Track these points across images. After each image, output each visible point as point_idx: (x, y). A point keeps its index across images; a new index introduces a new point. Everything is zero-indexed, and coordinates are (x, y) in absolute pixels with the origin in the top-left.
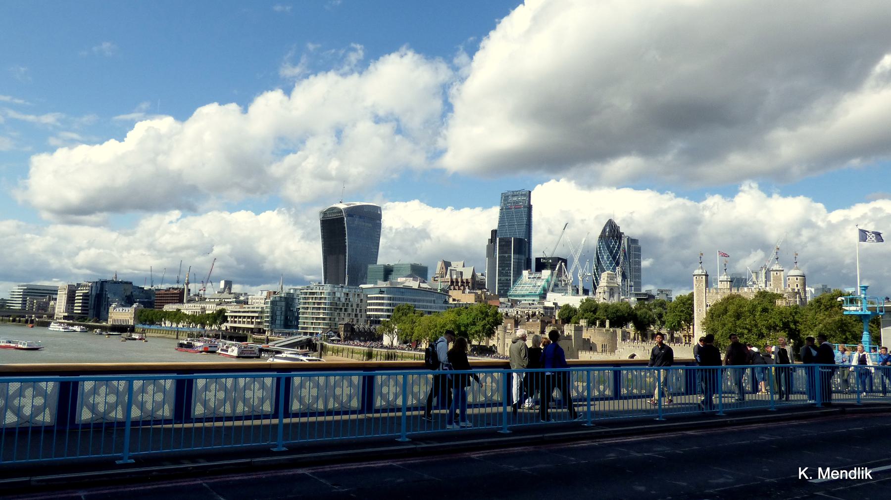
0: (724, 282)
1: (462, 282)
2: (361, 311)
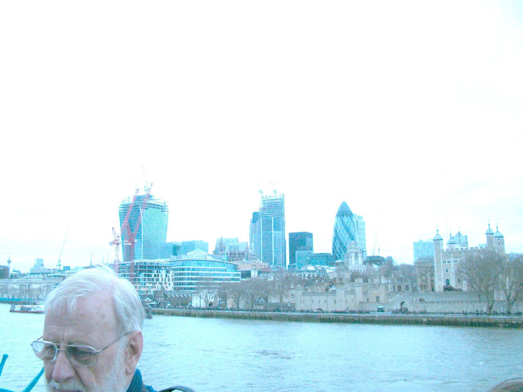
1: (239, 254)
2: (169, 280)
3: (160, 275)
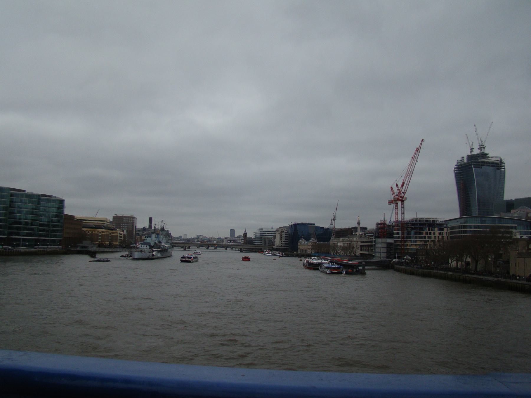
3: (432, 232)
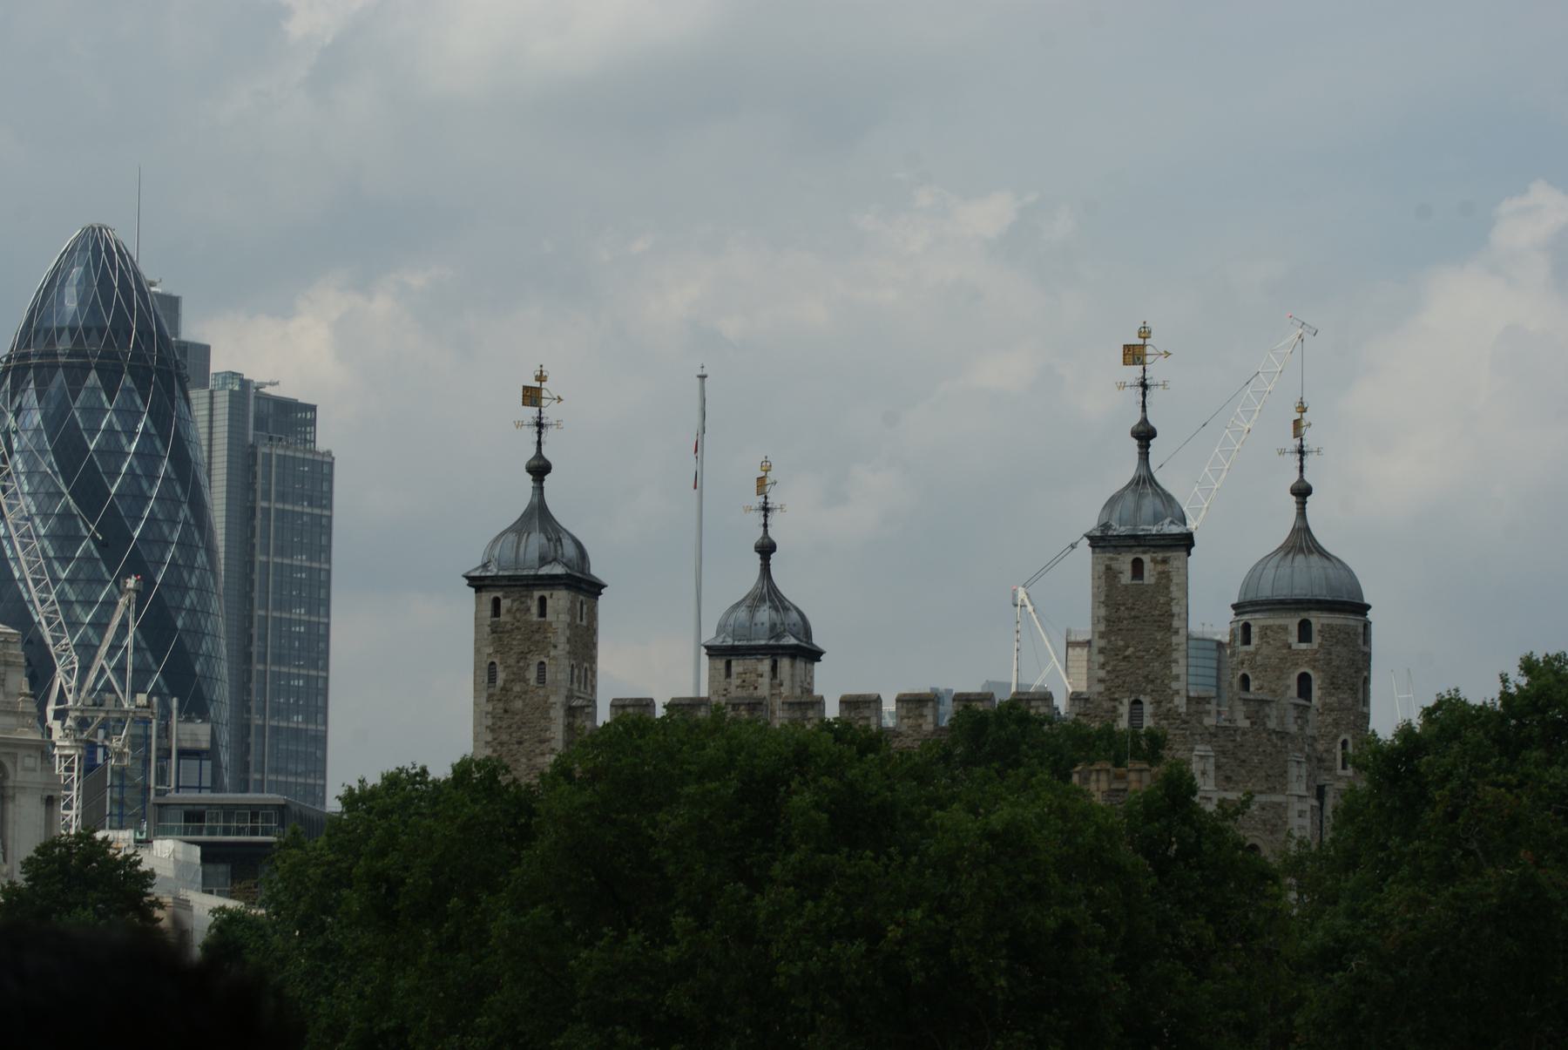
0: (750, 663)
